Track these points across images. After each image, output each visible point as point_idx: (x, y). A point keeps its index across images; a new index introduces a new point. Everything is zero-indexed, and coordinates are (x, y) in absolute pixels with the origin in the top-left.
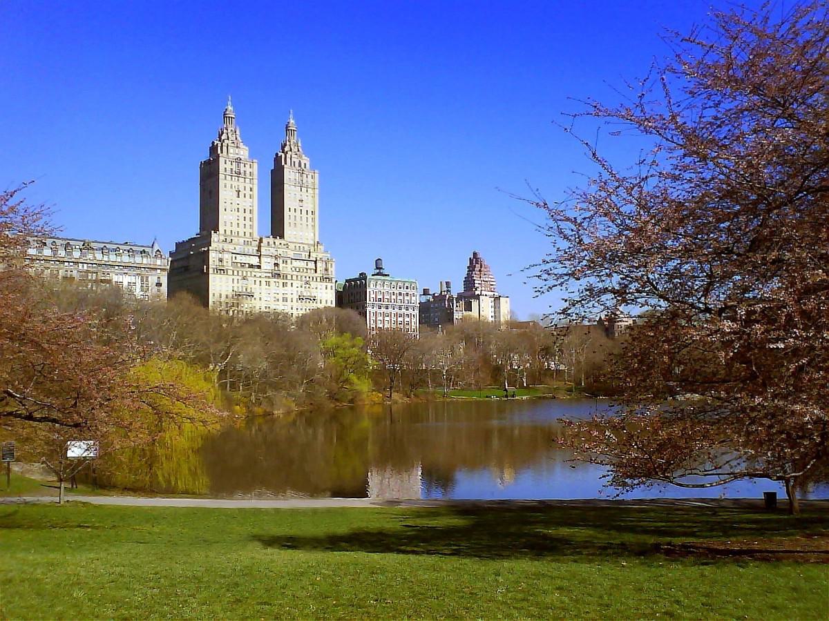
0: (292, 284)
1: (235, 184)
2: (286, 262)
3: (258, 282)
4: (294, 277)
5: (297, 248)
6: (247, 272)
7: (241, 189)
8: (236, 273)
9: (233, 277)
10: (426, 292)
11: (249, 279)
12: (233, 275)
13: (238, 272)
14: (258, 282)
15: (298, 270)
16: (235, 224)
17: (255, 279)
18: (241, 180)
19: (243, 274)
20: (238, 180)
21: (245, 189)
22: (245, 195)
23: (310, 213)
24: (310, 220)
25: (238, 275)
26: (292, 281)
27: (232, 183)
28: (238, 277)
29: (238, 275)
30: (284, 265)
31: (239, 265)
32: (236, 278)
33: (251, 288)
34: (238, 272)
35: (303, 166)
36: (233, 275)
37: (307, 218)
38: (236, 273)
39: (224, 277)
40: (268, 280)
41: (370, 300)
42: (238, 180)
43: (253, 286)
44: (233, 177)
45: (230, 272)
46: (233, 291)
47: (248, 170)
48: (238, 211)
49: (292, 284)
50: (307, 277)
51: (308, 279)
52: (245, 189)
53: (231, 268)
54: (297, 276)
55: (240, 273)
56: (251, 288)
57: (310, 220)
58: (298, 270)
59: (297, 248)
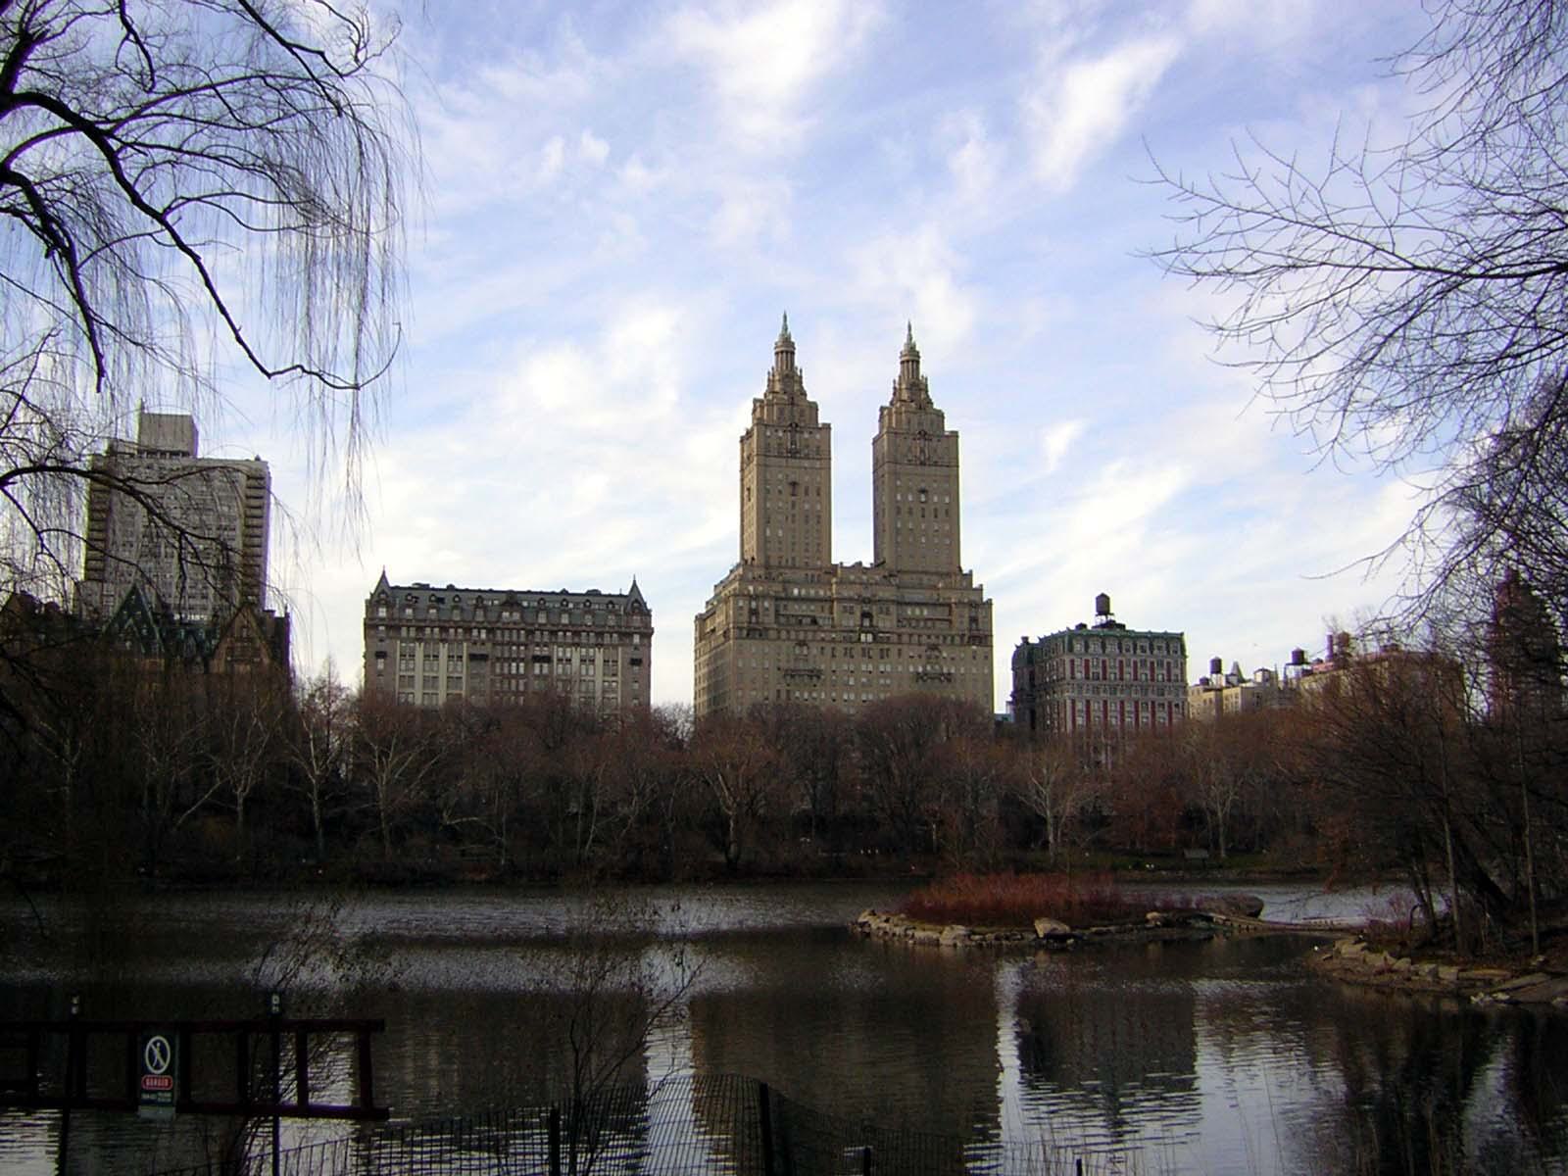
0: (900, 650)
2: (888, 609)
3: (828, 651)
4: (905, 638)
9: (779, 642)
10: (1299, 657)
11: (810, 645)
12: (779, 638)
17: (823, 645)
26: (900, 646)
38: (784, 634)
40: (849, 645)
41: (1073, 678)
45: (772, 634)
48: (793, 522)
49: (900, 650)
51: (933, 640)
53: (775, 626)
55: (793, 635)
58: (914, 624)
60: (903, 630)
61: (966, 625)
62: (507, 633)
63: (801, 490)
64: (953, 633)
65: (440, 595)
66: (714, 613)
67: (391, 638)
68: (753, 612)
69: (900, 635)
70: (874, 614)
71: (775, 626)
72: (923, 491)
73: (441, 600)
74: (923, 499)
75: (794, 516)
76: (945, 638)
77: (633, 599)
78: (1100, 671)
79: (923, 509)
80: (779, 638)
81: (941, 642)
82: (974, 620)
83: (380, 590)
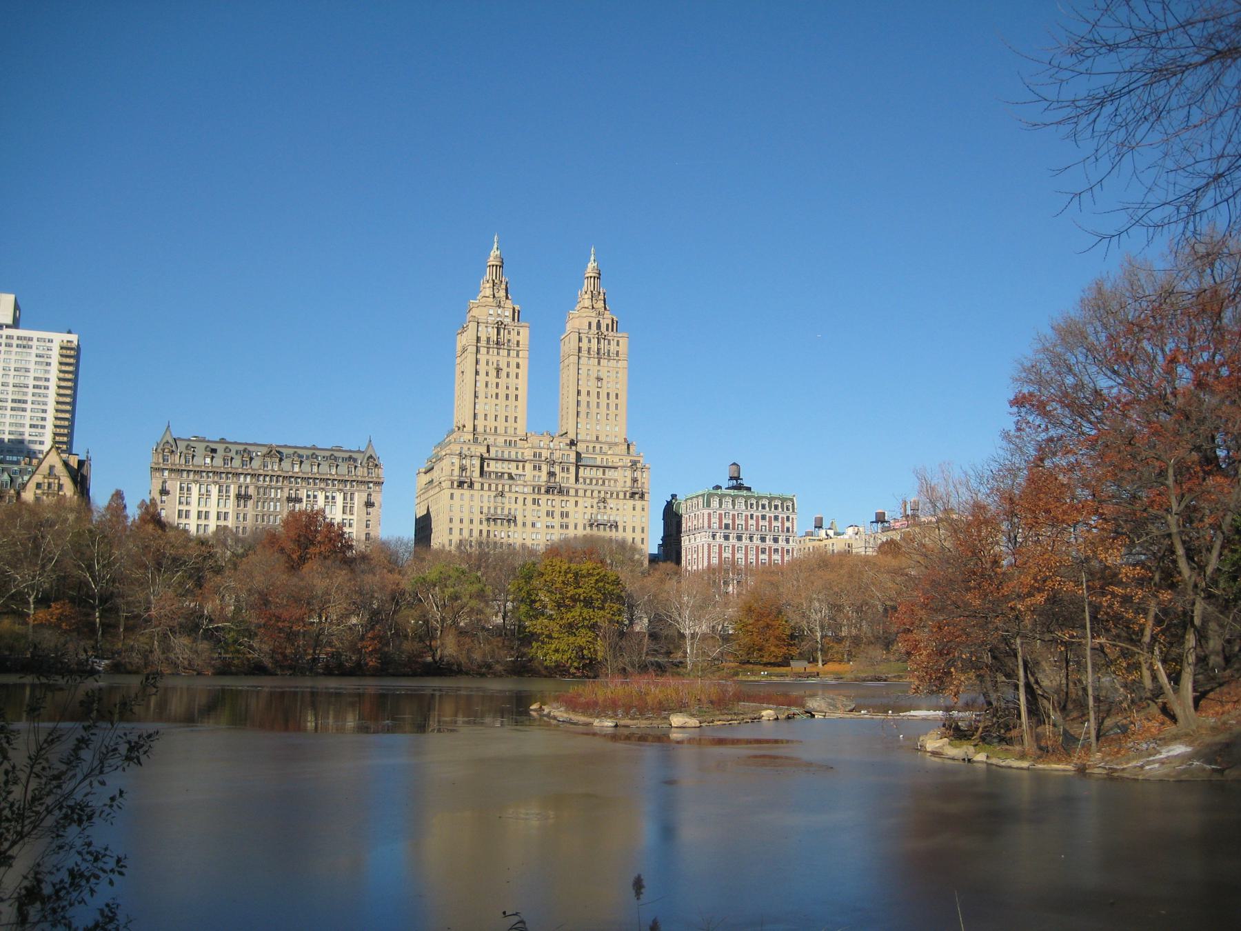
0: (576, 502)
1: (495, 359)
2: (568, 469)
3: (520, 501)
4: (581, 493)
5: (591, 449)
6: (610, 486)
7: (503, 365)
8: (486, 486)
9: (482, 492)
10: (880, 518)
13: (490, 485)
14: (520, 501)
15: (588, 481)
16: (491, 417)
18: (504, 352)
19: (497, 489)
20: (498, 354)
21: (508, 365)
22: (508, 376)
23: (612, 396)
24: (612, 407)
25: (490, 489)
26: (576, 499)
27: (488, 357)
28: (489, 493)
29: (490, 489)
30: (565, 475)
31: (493, 476)
32: (486, 494)
33: (510, 509)
34: (490, 485)
35: (603, 328)
36: (482, 489)
37: (608, 404)
38: (486, 486)
39: (466, 492)
42: (498, 354)
43: (513, 506)
44: (491, 350)
45: (477, 486)
46: (481, 513)
47: (514, 337)
49: (576, 502)
50: (602, 493)
52: (508, 365)
54: (585, 491)
56: (510, 509)
57: (612, 407)
58: (588, 481)
59: (591, 449)
60: (579, 486)
61: (629, 483)
62: (268, 479)
63: (503, 374)
64: (619, 489)
65: (213, 446)
66: (433, 468)
67: (172, 479)
68: (463, 469)
69: (577, 491)
70: (557, 472)
71: (480, 480)
72: (599, 379)
73: (214, 451)
74: (600, 385)
75: (497, 395)
76: (612, 494)
77: (368, 455)
78: (730, 522)
79: (598, 393)
80: (482, 489)
81: (609, 496)
82: (635, 480)
83: (164, 441)
